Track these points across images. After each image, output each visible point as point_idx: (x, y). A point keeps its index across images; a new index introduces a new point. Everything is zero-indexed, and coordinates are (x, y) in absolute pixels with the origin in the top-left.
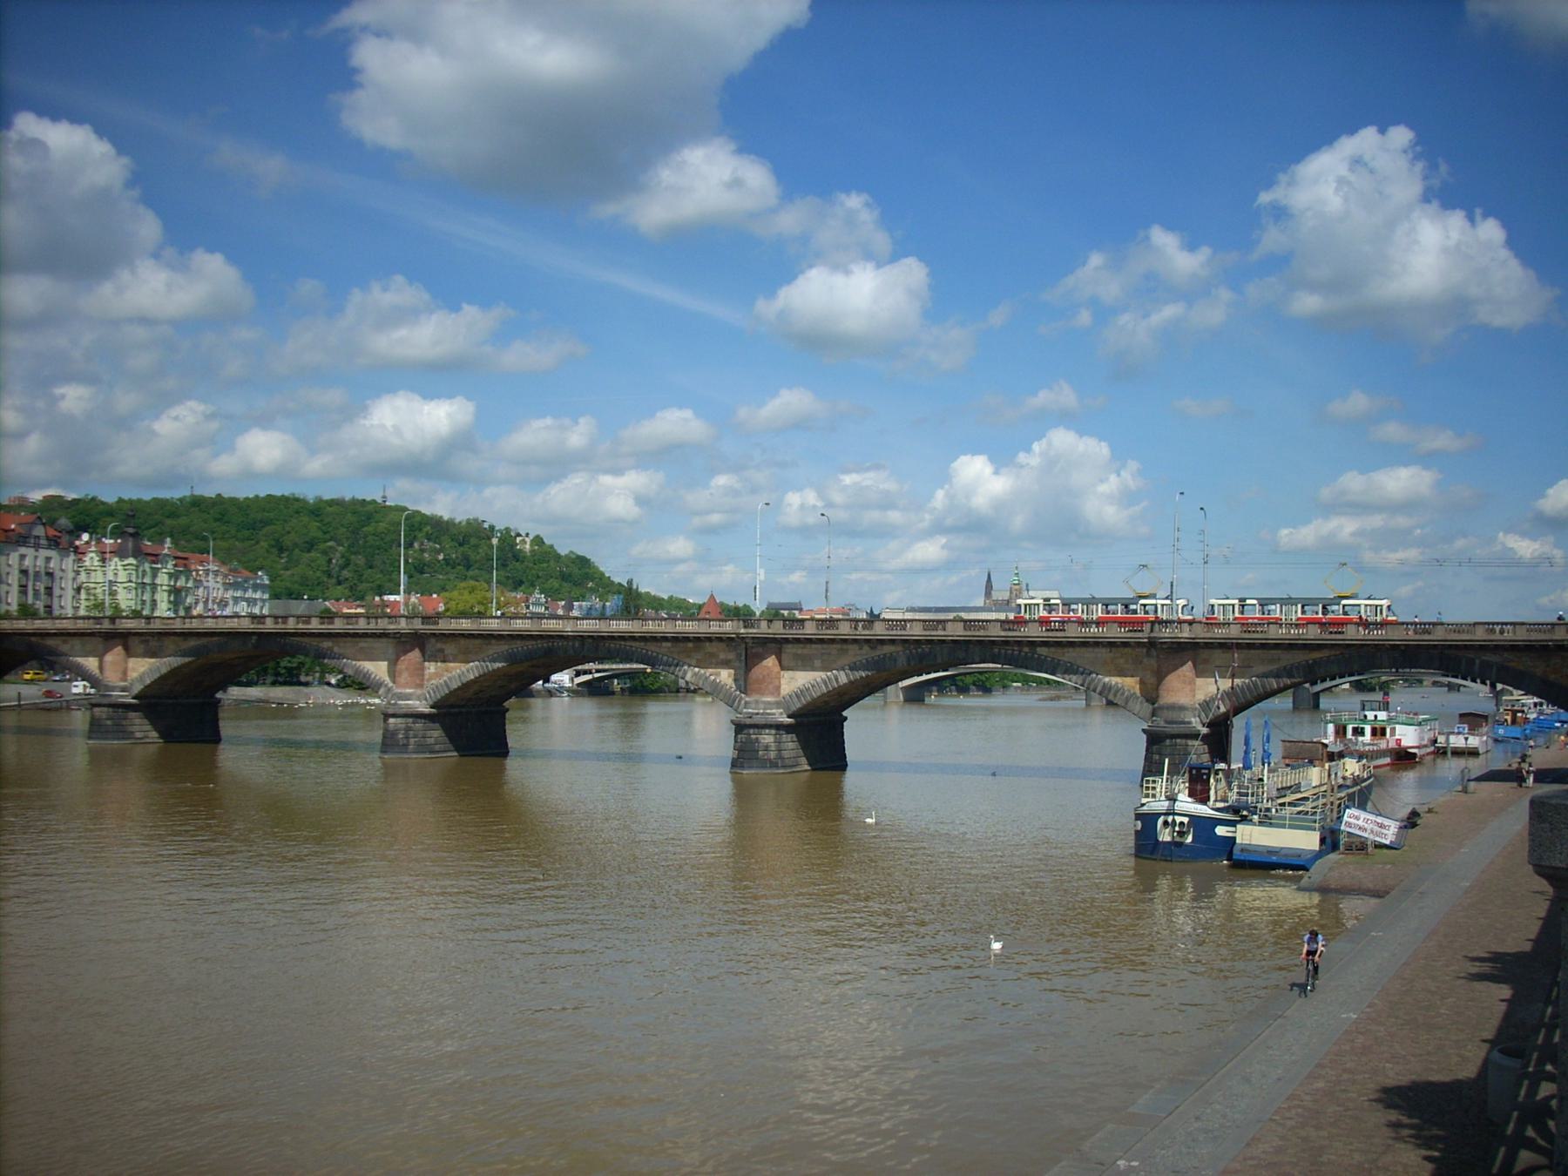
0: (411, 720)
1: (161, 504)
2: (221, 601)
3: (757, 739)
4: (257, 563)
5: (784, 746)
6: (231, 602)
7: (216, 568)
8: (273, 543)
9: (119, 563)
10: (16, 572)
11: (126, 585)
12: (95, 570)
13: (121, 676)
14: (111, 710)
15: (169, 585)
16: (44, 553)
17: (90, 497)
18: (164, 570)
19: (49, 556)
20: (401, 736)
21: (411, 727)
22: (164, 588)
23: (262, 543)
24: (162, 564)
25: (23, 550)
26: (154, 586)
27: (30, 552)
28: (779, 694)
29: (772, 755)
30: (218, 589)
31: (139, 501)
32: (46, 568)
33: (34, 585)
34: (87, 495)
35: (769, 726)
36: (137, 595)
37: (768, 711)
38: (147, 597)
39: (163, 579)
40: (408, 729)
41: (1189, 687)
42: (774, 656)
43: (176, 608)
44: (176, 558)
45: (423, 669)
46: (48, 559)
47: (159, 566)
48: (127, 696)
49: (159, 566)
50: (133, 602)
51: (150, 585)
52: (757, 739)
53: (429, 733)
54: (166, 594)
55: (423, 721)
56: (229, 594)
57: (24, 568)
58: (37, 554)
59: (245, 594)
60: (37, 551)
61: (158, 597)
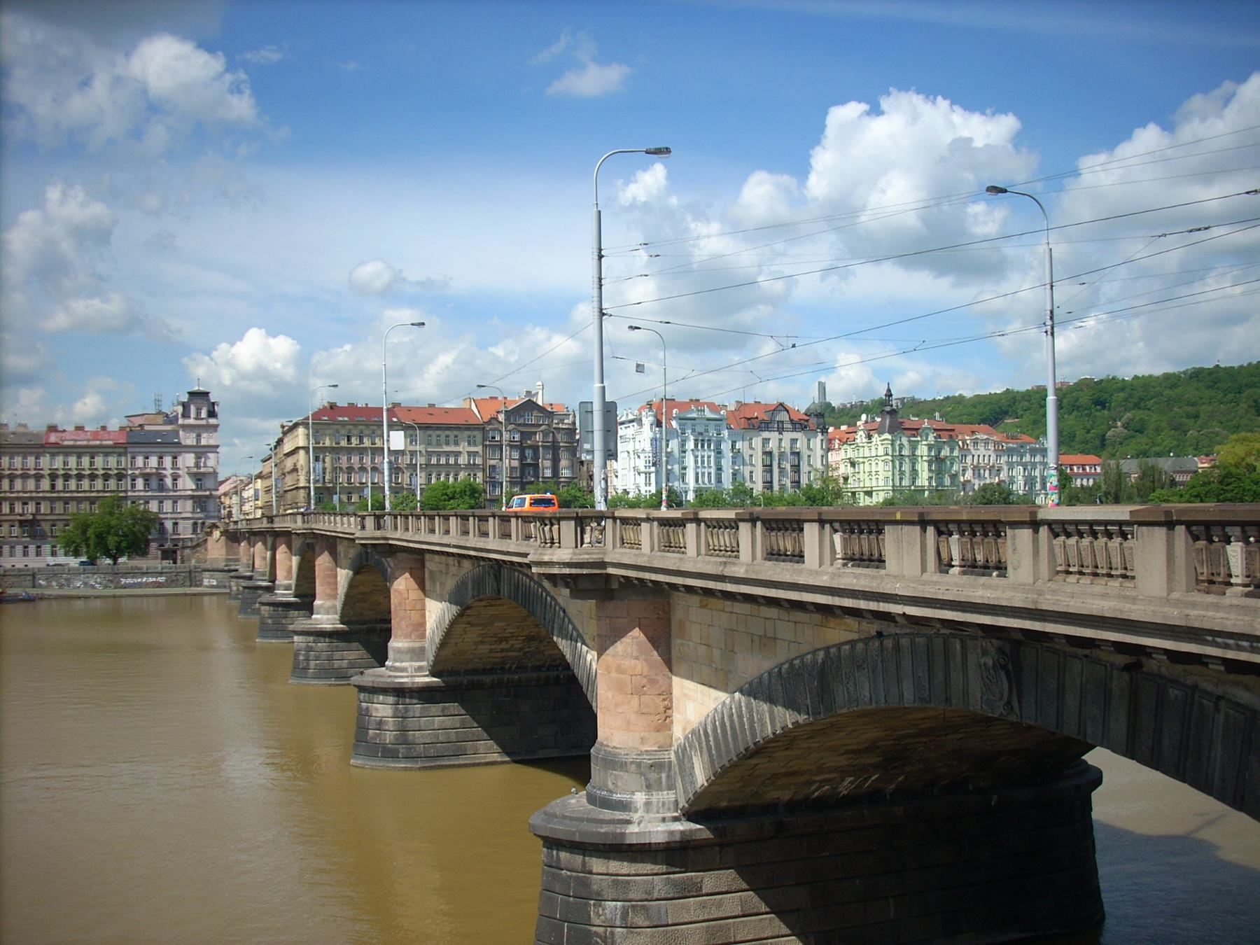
0: (311, 639)
1: (1167, 377)
2: (993, 466)
3: (367, 708)
4: (1234, 422)
5: (411, 723)
6: (1005, 468)
7: (985, 437)
8: (1254, 404)
9: (879, 439)
10: (760, 453)
11: (883, 458)
12: (863, 447)
13: (285, 574)
14: (271, 608)
15: (928, 456)
16: (788, 436)
17: (1110, 377)
18: (924, 443)
19: (768, 437)
20: (301, 658)
21: (312, 647)
22: (925, 458)
23: (1241, 405)
24: (921, 437)
25: (766, 435)
26: (914, 458)
27: (773, 436)
28: (423, 636)
29: (389, 737)
30: (990, 456)
31: (1150, 376)
32: (791, 448)
33: (779, 464)
34: (1108, 376)
35: (384, 691)
36: (894, 467)
37: (398, 664)
38: (906, 467)
39: (922, 450)
40: (309, 649)
41: (635, 701)
42: (407, 575)
43: (940, 476)
44: (935, 430)
45: (336, 576)
46: (794, 441)
47: (919, 439)
48: (290, 594)
49: (919, 439)
50: (890, 473)
51: (908, 456)
52: (367, 708)
53: (338, 655)
54: (926, 464)
55: (327, 640)
56: (1004, 459)
57: (768, 450)
58: (781, 436)
59: (1022, 459)
60: (781, 433)
61: (918, 467)
